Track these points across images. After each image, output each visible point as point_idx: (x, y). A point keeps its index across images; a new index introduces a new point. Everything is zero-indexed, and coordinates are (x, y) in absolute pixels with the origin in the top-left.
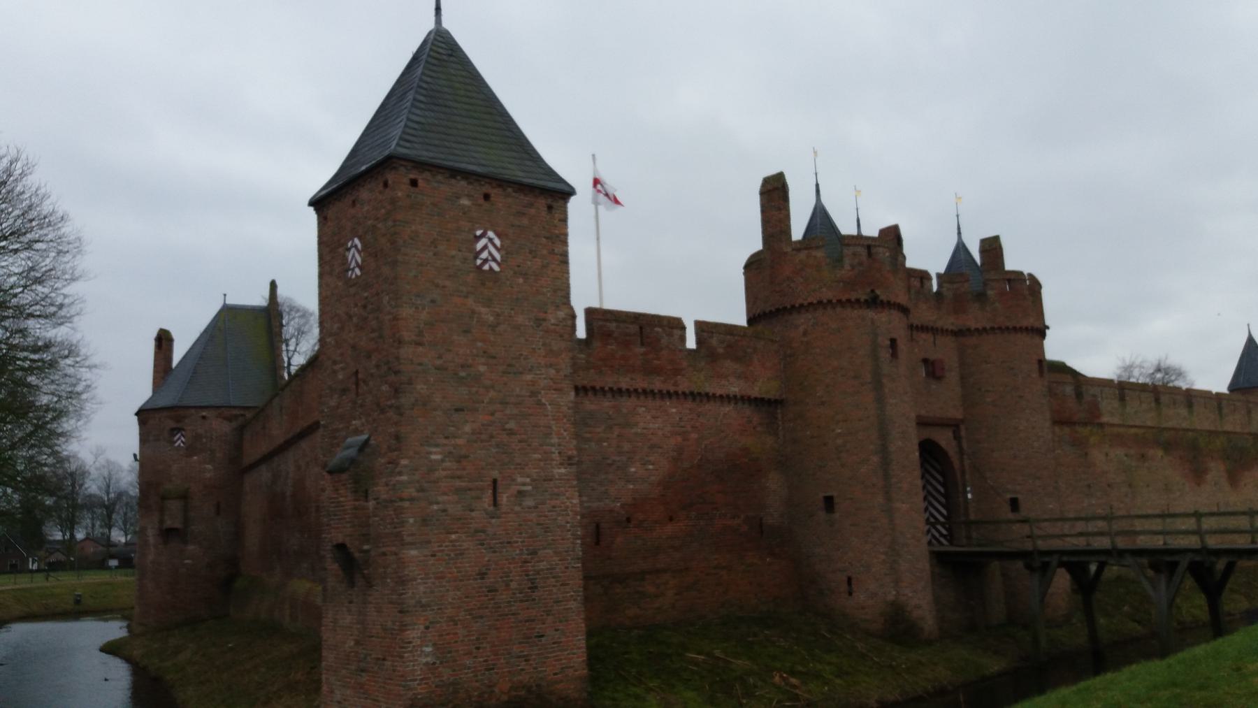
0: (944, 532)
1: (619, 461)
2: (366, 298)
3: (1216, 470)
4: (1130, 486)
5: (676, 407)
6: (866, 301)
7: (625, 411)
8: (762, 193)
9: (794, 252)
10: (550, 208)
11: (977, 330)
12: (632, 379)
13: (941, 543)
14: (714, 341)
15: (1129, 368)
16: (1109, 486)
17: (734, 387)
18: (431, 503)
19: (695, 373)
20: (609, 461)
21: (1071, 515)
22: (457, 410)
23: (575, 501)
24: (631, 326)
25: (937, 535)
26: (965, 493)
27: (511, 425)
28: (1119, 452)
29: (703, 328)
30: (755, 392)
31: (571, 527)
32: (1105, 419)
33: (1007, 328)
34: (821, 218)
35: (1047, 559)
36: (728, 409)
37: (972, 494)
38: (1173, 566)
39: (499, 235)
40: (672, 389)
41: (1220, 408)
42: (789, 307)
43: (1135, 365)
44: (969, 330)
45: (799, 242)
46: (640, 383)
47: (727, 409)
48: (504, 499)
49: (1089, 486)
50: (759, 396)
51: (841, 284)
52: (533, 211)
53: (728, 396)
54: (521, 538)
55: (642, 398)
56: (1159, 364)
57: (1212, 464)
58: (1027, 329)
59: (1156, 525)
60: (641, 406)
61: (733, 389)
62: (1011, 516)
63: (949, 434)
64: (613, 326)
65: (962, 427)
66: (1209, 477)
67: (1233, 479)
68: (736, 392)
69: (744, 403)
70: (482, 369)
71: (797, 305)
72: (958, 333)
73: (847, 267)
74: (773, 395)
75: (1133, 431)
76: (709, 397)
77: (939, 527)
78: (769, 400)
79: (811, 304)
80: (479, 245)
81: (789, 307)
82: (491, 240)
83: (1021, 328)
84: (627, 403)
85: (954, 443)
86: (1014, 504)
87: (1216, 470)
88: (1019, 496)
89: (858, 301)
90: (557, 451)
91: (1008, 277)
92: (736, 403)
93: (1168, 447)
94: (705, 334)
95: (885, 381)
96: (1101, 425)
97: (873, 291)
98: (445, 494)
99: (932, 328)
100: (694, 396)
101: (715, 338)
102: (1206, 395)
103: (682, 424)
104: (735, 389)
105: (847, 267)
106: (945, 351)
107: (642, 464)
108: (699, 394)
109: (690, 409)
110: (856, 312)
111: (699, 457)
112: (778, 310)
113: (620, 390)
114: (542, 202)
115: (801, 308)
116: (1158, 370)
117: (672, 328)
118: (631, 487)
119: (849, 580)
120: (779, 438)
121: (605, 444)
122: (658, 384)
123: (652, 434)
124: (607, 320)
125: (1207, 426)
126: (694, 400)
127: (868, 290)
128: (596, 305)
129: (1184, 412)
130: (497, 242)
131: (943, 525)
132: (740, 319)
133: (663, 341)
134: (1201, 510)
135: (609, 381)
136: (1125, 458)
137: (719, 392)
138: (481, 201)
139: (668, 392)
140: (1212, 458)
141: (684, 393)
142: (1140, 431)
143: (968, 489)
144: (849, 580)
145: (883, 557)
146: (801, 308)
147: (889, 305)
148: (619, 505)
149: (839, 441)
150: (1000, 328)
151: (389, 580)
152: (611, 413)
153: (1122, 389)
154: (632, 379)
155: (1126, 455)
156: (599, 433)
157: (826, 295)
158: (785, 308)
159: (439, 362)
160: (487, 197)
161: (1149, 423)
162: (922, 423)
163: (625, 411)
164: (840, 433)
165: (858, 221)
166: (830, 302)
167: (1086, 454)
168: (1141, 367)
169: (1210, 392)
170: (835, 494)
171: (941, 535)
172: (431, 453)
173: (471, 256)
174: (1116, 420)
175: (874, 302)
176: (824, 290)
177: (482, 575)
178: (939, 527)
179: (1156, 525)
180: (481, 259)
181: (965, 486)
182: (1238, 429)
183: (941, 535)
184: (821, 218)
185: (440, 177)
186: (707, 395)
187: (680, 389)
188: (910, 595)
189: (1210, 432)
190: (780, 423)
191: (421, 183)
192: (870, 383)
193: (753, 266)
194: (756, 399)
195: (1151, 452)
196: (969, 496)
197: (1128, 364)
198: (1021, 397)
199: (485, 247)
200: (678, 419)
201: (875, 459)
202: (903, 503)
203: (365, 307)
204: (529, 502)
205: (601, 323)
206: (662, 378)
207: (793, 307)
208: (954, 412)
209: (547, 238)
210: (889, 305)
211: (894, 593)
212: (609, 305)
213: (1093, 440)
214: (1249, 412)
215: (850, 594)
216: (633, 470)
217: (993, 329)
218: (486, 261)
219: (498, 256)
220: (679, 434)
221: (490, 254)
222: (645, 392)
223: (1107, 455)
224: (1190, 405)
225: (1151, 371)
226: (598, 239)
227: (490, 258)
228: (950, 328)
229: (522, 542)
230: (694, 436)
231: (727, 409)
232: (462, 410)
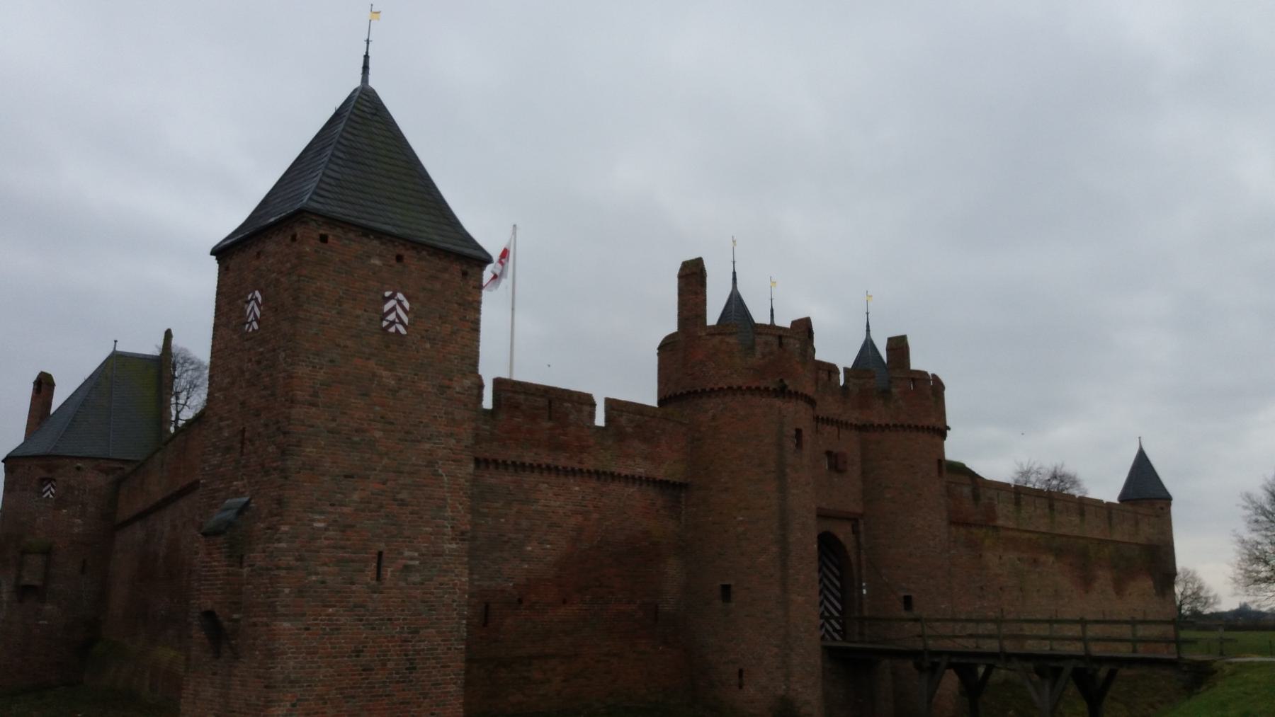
0: (838, 627)
1: (515, 539)
2: (262, 353)
3: (1104, 577)
4: (1021, 590)
5: (579, 486)
6: (775, 389)
7: (526, 486)
8: (681, 277)
9: (708, 337)
10: (465, 274)
11: (880, 426)
12: (536, 454)
13: (834, 639)
14: (623, 420)
15: (1025, 474)
16: (1001, 589)
17: (640, 468)
18: (310, 574)
19: (601, 451)
20: (506, 539)
21: (963, 617)
22: (346, 477)
23: (463, 579)
24: (539, 399)
25: (830, 629)
26: (861, 588)
27: (404, 495)
29: (613, 406)
30: (660, 474)
31: (457, 606)
32: (1000, 522)
33: (909, 426)
34: (735, 304)
35: (936, 660)
36: (631, 490)
37: (867, 590)
38: (1057, 672)
39: (408, 298)
40: (577, 466)
41: (1110, 518)
42: (699, 390)
43: (1032, 471)
44: (872, 425)
45: (713, 327)
46: (546, 459)
47: (632, 490)
48: (388, 573)
49: (982, 588)
50: (664, 479)
51: (752, 371)
52: (446, 276)
53: (633, 477)
54: (402, 615)
55: (545, 473)
56: (1055, 471)
58: (928, 428)
59: (1043, 630)
60: (544, 483)
61: (639, 470)
62: (904, 614)
63: (847, 527)
64: (521, 397)
65: (861, 522)
67: (1119, 588)
68: (641, 473)
69: (649, 485)
70: (378, 434)
71: (707, 389)
72: (862, 428)
73: (758, 355)
74: (677, 478)
75: (1027, 535)
76: (614, 477)
77: (833, 622)
78: (674, 483)
79: (721, 389)
80: (387, 307)
81: (699, 390)
82: (400, 302)
83: (923, 427)
84: (529, 479)
86: (908, 602)
87: (1104, 577)
88: (914, 595)
89: (767, 389)
90: (449, 526)
91: (912, 376)
92: (641, 485)
94: (615, 413)
95: (788, 470)
96: (996, 528)
97: (781, 381)
98: (325, 564)
99: (837, 421)
100: (598, 475)
101: (624, 417)
102: (1098, 504)
103: (584, 503)
104: (640, 471)
105: (758, 355)
106: (849, 444)
107: (539, 543)
108: (604, 473)
109: (594, 488)
110: (764, 400)
111: (599, 539)
112: (689, 393)
113: (523, 464)
114: (456, 268)
115: (712, 392)
116: (1054, 477)
117: (582, 404)
118: (526, 566)
119: (741, 672)
120: (681, 523)
121: (503, 520)
122: (562, 461)
123: (553, 512)
124: (515, 392)
125: (1097, 534)
126: (599, 479)
127: (778, 379)
128: (505, 375)
129: (1076, 519)
130: (407, 304)
131: (837, 619)
132: (651, 399)
133: (571, 417)
134: (1088, 617)
135: (512, 455)
136: (1019, 562)
137: (624, 472)
138: (393, 262)
139: (573, 470)
141: (589, 471)
143: (864, 584)
144: (741, 672)
145: (776, 650)
146: (712, 392)
147: (796, 395)
148: (511, 585)
149: (740, 529)
150: (902, 426)
151: (257, 653)
152: (511, 488)
153: (1018, 494)
154: (536, 454)
155: (1019, 559)
156: (497, 508)
157: (737, 381)
158: (696, 392)
159: (333, 425)
160: (399, 258)
161: (1043, 529)
162: (822, 515)
163: (526, 486)
164: (741, 521)
165: (772, 311)
166: (740, 388)
167: (981, 556)
168: (1038, 473)
169: (1100, 502)
170: (732, 583)
171: (835, 630)
172: (314, 520)
173: (378, 317)
174: (1011, 524)
175: (782, 392)
176: (735, 376)
177: (358, 653)
178: (833, 622)
179: (1043, 630)
180: (387, 321)
181: (860, 582)
182: (1126, 539)
183: (835, 630)
184: (735, 304)
185: (351, 235)
186: (612, 474)
187: (585, 467)
188: (800, 690)
189: (1100, 541)
190: (683, 507)
191: (330, 238)
192: (774, 472)
193: (667, 347)
194: (661, 481)
196: (865, 592)
197: (1025, 468)
199: (393, 309)
200: (580, 498)
201: (774, 549)
202: (799, 595)
203: (259, 362)
204: (416, 578)
205: (509, 395)
206: (568, 455)
207: (704, 390)
208: (855, 507)
209: (459, 304)
210: (796, 395)
211: (784, 687)
212: (519, 376)
215: (741, 687)
216: (529, 548)
217: (895, 426)
218: (392, 323)
219: (405, 319)
220: (581, 514)
221: (398, 316)
222: (548, 468)
223: (1000, 558)
224: (1082, 514)
225: (1047, 478)
226: (513, 309)
227: (397, 320)
228: (855, 422)
229: (404, 619)
230: (595, 516)
231: (632, 490)
232: (352, 477)
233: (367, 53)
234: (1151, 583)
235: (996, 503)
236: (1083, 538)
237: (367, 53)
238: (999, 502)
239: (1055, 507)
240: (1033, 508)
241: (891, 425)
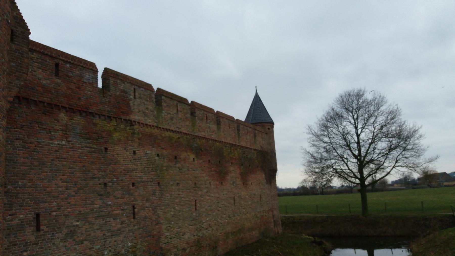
16: (133, 184)
28: (151, 152)
32: (135, 117)
49: (105, 184)
57: (232, 169)
66: (229, 178)
67: (244, 179)
75: (168, 134)
93: (199, 152)
96: (131, 123)
102: (230, 119)
125: (229, 140)
129: (213, 127)
136: (157, 158)
140: (232, 163)
142: (176, 136)
155: (158, 155)
161: (184, 130)
167: (106, 149)
169: (233, 118)
174: (149, 121)
189: (232, 145)
195: (184, 155)
213: (116, 135)
214: (255, 136)
223: (134, 152)
224: (218, 123)
234: (264, 176)
235: (132, 97)
236: (219, 142)
238: (135, 98)
239: (196, 114)
240: (175, 112)
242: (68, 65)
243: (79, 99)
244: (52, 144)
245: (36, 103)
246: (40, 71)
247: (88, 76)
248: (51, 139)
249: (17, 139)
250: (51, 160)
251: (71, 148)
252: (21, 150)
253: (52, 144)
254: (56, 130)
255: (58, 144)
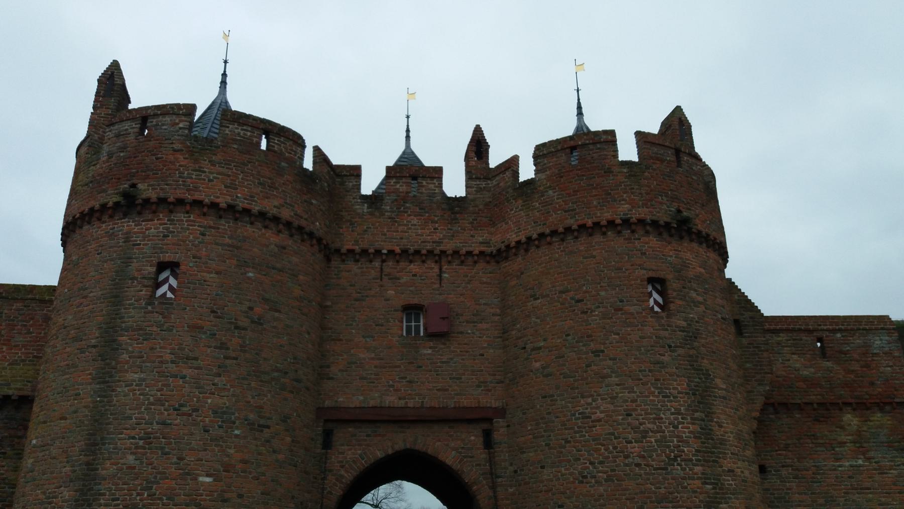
63: (473, 437)
65: (499, 422)
72: (501, 255)
85: (481, 455)
150: (554, 233)
198: (597, 353)
217: (542, 235)
233: (225, 71)
237: (225, 71)
241: (535, 236)
242: (839, 335)
243: (872, 384)
244: (840, 466)
245: (800, 407)
246: (795, 357)
247: (878, 342)
248: (837, 460)
249: (783, 466)
250: (845, 493)
251: (875, 469)
252: (792, 482)
253: (840, 466)
254: (842, 444)
255: (851, 466)
